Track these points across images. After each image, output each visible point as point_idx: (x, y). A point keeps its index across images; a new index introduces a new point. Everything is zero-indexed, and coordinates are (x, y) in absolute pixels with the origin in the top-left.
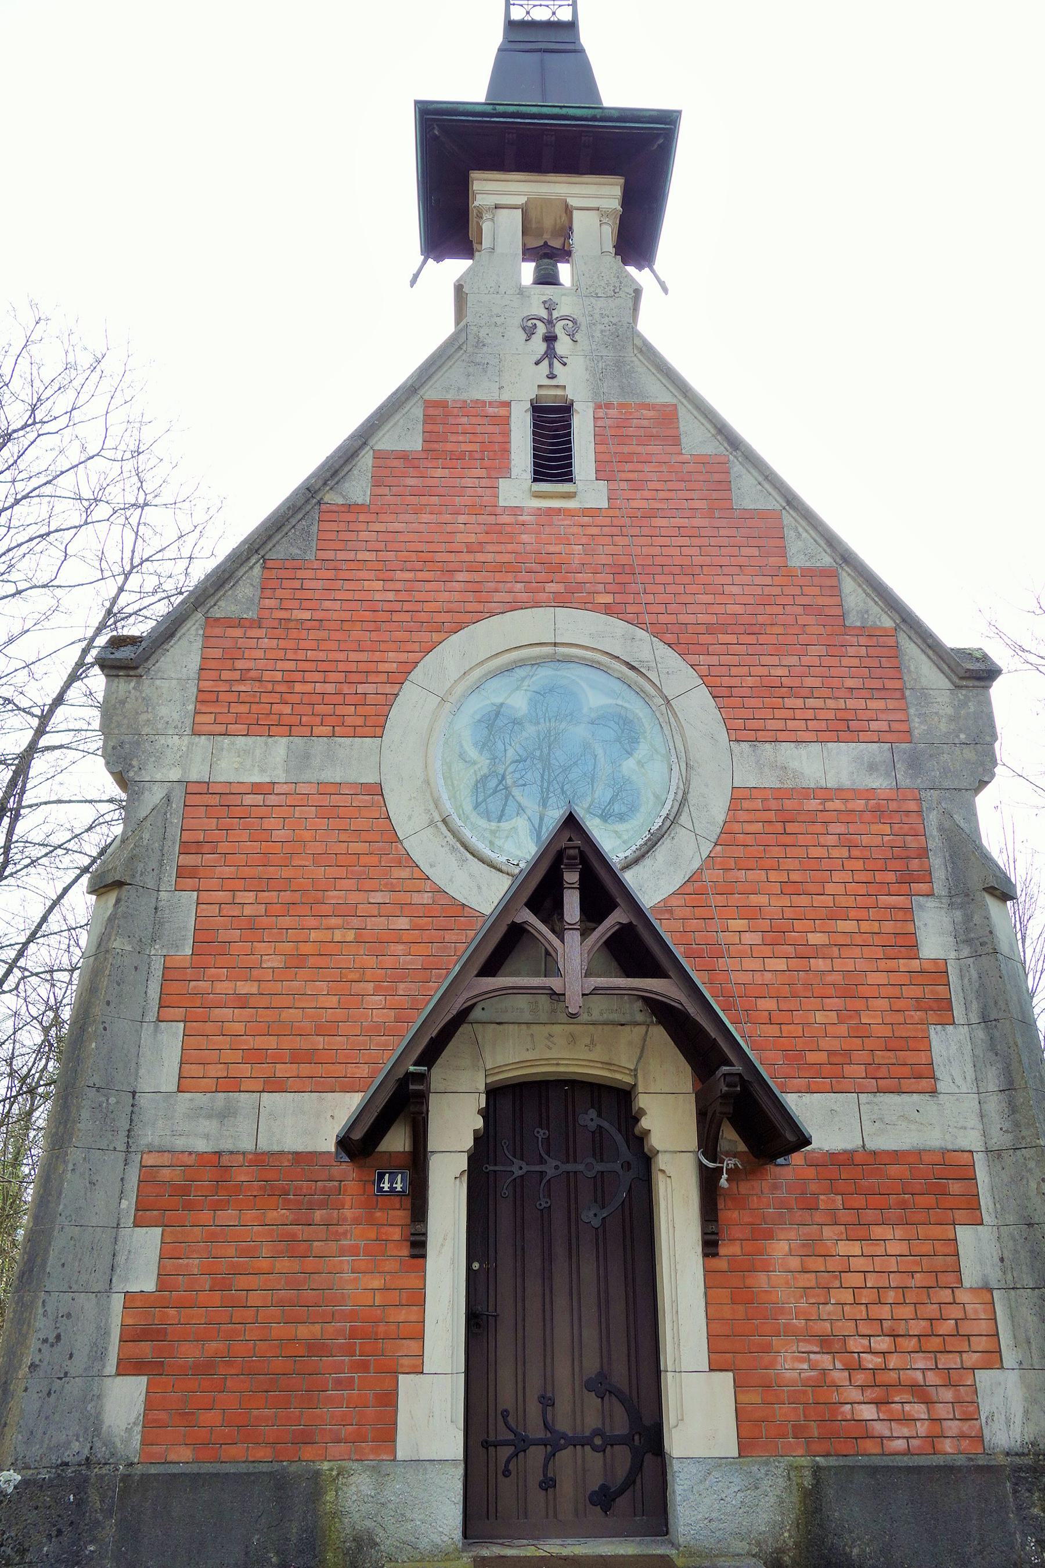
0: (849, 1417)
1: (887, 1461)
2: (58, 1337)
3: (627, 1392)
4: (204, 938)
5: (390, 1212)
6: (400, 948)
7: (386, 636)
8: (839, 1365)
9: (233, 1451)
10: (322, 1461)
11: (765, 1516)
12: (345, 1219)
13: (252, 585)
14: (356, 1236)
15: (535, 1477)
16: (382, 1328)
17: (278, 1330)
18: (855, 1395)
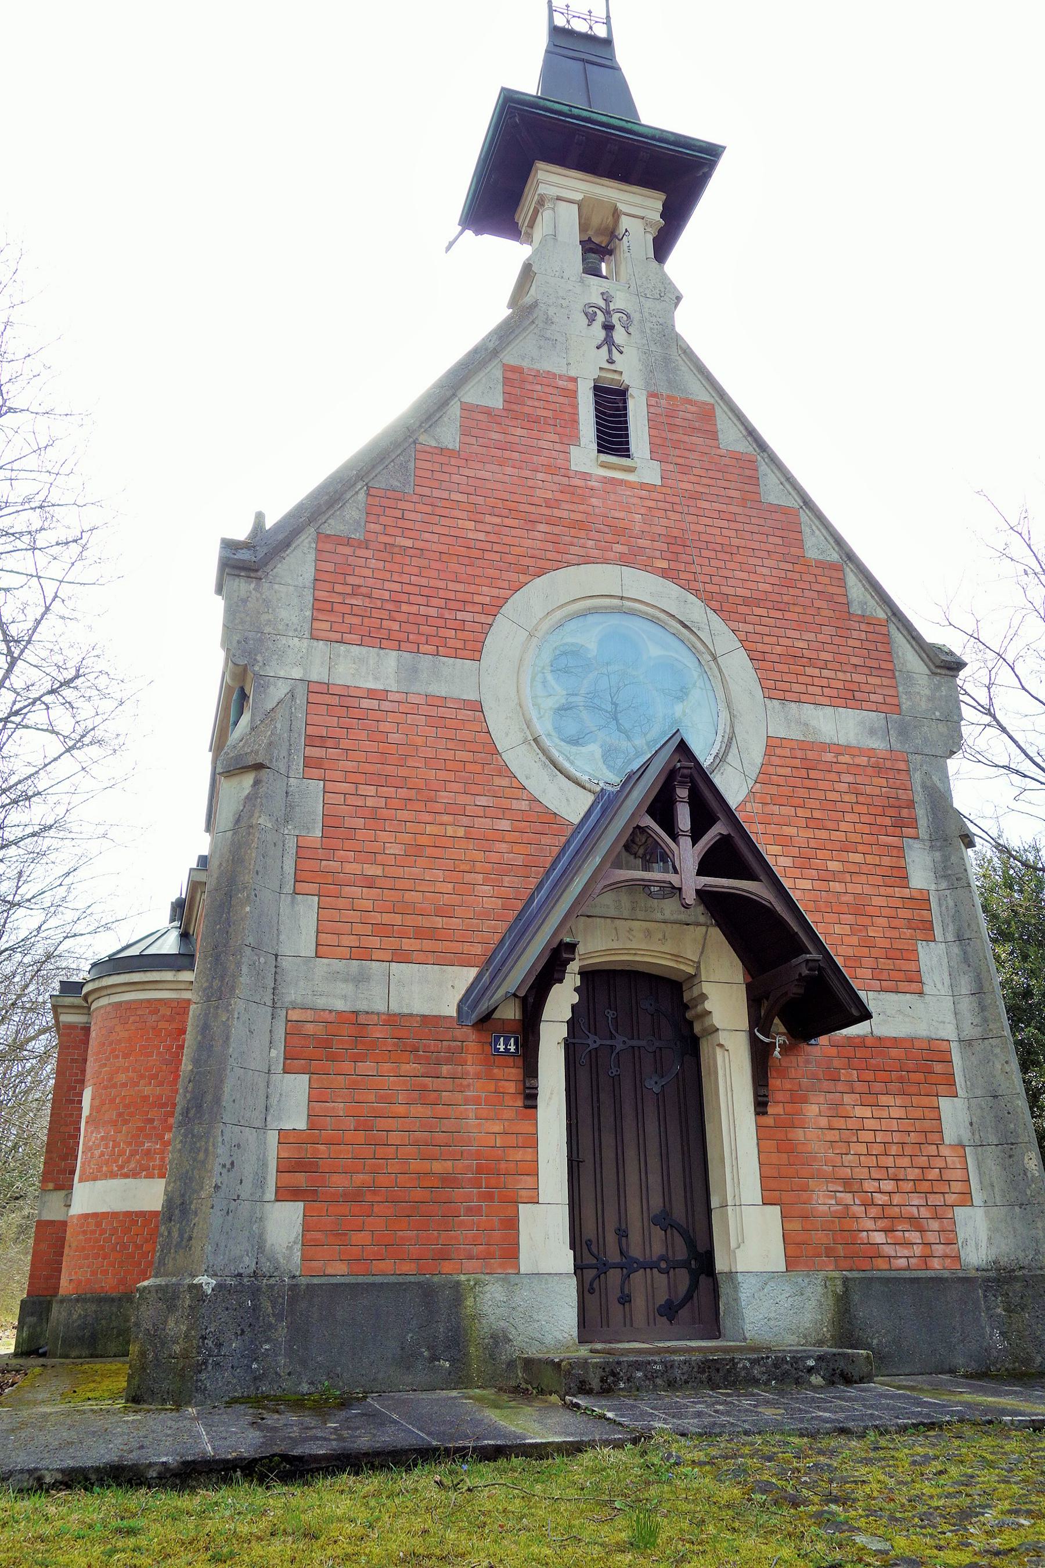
0: (866, 1242)
1: (893, 1274)
2: (232, 1163)
3: (685, 1226)
4: (331, 823)
5: (506, 1069)
6: (503, 847)
7: (478, 571)
8: (857, 1202)
9: (382, 1265)
10: (458, 1274)
11: (809, 1316)
12: (468, 1073)
13: (357, 508)
14: (477, 1089)
15: (614, 1294)
16: (503, 1165)
17: (415, 1165)
18: (869, 1224)
